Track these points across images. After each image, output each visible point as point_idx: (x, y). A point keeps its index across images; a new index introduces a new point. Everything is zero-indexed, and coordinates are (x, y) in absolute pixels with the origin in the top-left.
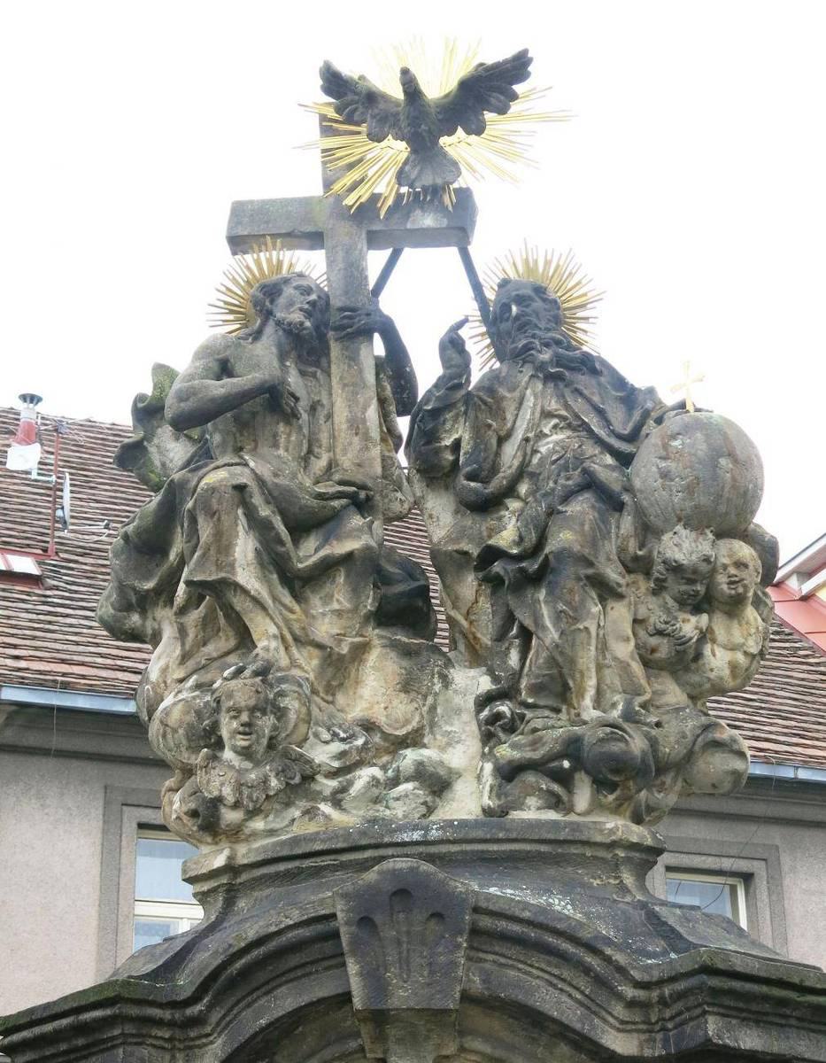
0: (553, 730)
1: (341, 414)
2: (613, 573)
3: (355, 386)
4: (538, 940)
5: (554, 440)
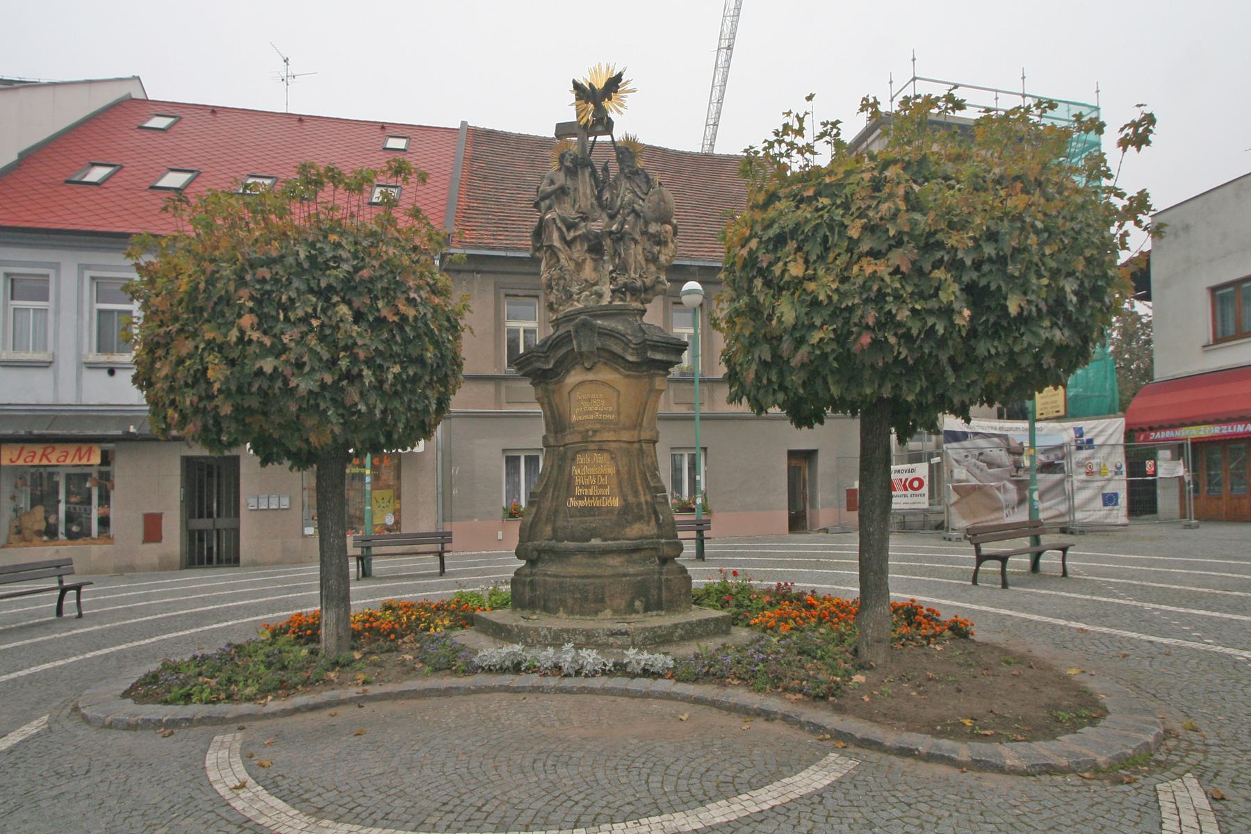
0: (622, 280)
1: (581, 191)
2: (637, 237)
3: (584, 182)
4: (611, 334)
5: (629, 196)
